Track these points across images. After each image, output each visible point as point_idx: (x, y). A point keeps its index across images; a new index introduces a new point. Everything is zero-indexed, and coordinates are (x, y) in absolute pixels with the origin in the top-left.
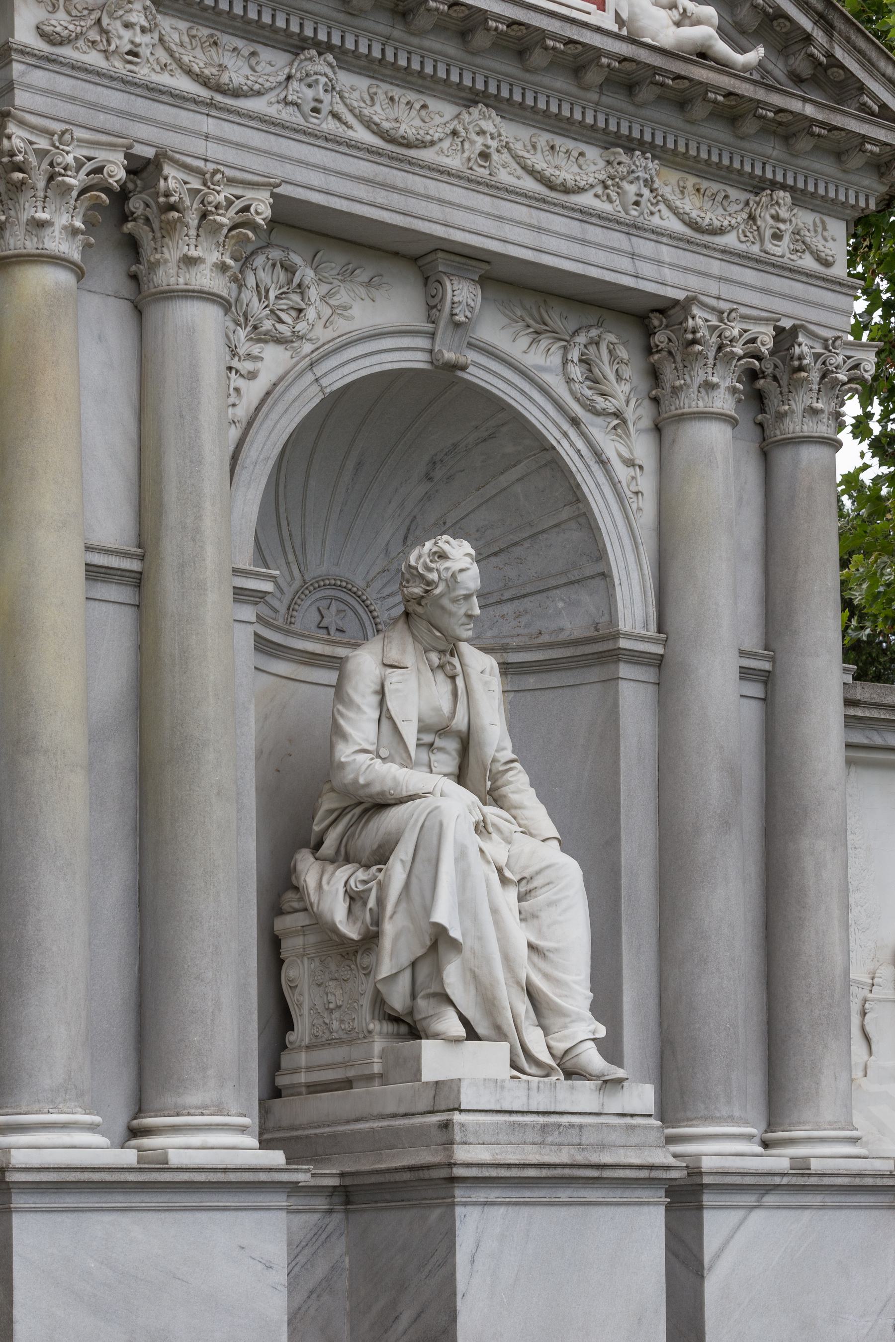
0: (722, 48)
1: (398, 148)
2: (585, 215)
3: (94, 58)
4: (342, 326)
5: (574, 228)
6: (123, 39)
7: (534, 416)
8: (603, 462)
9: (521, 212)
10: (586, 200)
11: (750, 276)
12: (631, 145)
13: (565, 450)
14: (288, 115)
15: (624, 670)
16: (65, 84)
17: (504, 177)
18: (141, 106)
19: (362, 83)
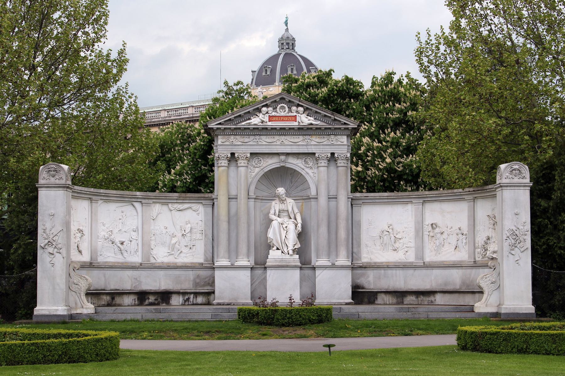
0: (313, 123)
1: (270, 144)
2: (299, 145)
3: (228, 143)
4: (268, 164)
5: (297, 147)
6: (231, 141)
7: (297, 169)
8: (308, 174)
9: (289, 147)
10: (300, 143)
11: (328, 147)
12: (305, 135)
13: (302, 173)
14: (254, 143)
15: (312, 200)
16: (224, 147)
17: (286, 143)
18: (233, 147)
19: (265, 137)
